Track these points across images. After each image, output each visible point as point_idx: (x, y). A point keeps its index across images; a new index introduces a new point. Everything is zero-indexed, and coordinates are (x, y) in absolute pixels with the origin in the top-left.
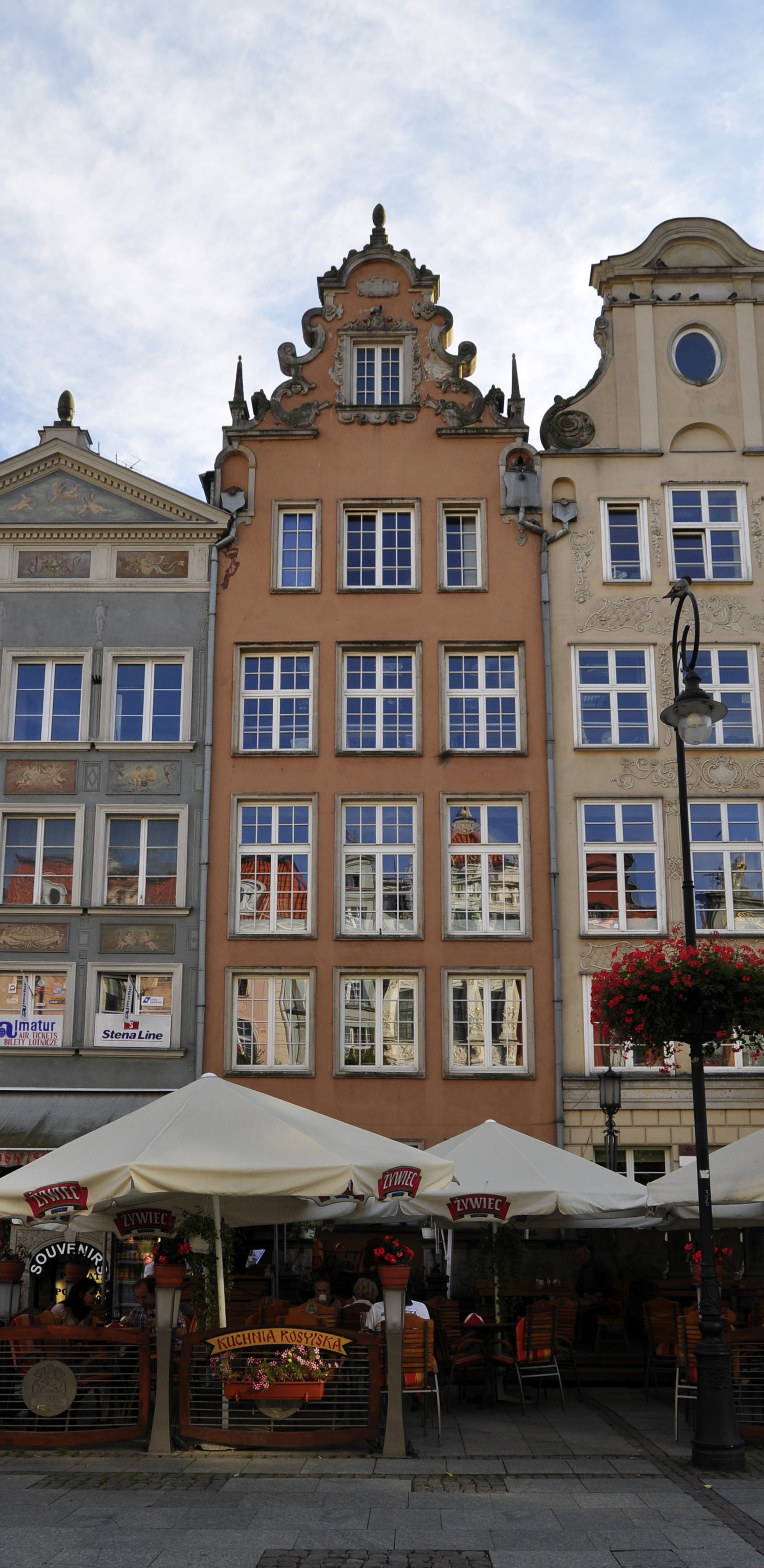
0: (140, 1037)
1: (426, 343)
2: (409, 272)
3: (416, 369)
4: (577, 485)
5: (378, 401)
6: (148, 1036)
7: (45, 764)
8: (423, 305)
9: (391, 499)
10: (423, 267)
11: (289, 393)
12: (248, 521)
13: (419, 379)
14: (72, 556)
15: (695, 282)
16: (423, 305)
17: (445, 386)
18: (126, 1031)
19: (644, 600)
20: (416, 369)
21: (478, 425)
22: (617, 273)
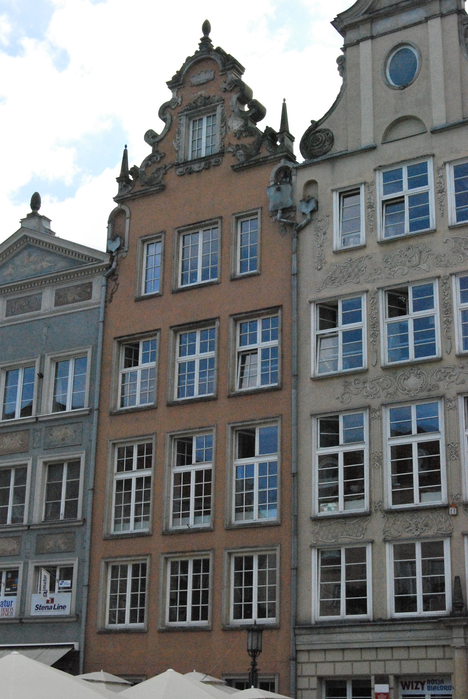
0: (54, 609)
3: (223, 127)
4: (319, 184)
6: (58, 608)
7: (14, 434)
8: (227, 82)
11: (150, 163)
12: (124, 254)
13: (224, 134)
14: (33, 298)
16: (227, 82)
17: (239, 135)
18: (47, 605)
19: (360, 260)
20: (223, 127)
21: (258, 157)
22: (345, 23)
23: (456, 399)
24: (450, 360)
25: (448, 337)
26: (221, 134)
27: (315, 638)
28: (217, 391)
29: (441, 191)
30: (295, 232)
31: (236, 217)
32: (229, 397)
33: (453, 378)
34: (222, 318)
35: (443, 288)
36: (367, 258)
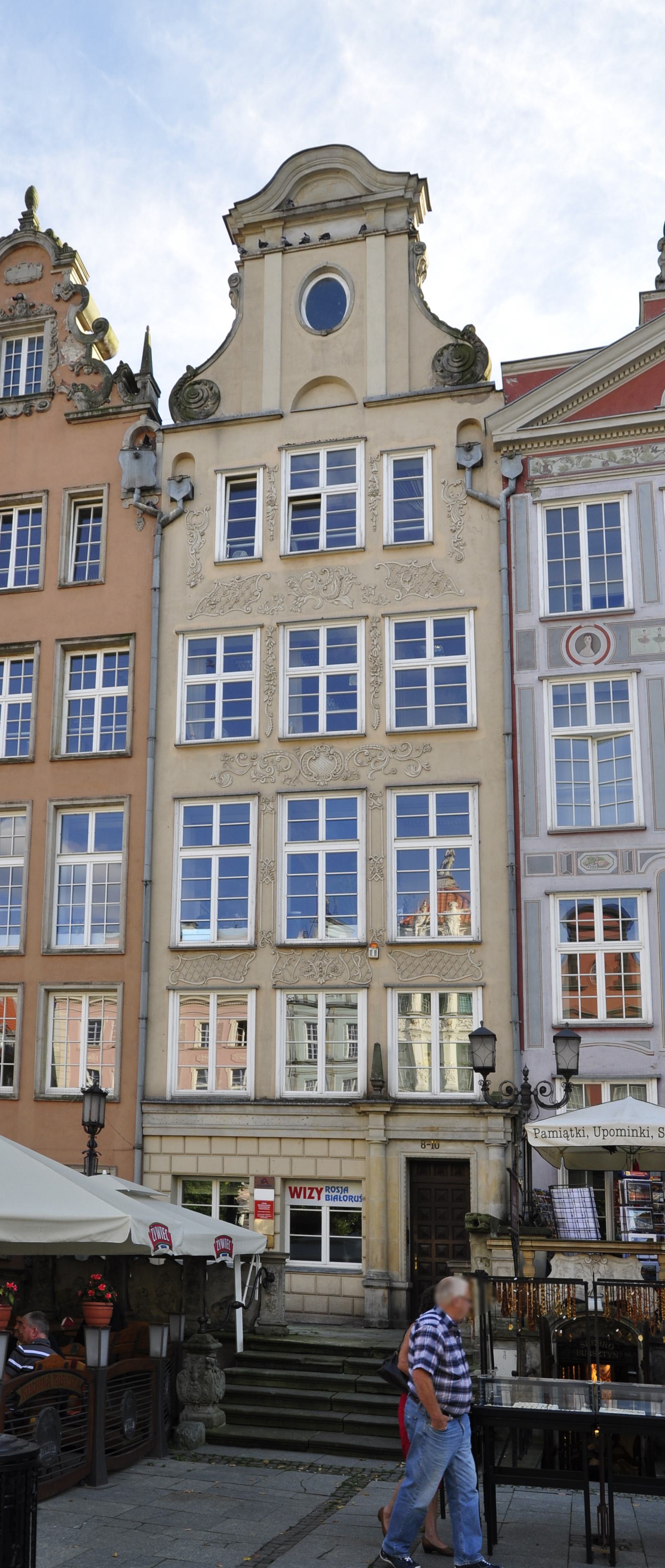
1: (63, 327)
2: (51, 252)
3: (53, 354)
5: (22, 392)
8: (62, 285)
9: (21, 494)
10: (65, 244)
15: (328, 221)
16: (62, 285)
17: (77, 369)
20: (53, 354)
21: (106, 405)
23: (383, 795)
24: (378, 739)
25: (375, 706)
26: (50, 365)
27: (171, 1119)
28: (34, 752)
29: (374, 493)
30: (159, 526)
31: (70, 495)
32: (52, 761)
33: (381, 766)
34: (44, 643)
35: (372, 634)
36: (263, 579)
